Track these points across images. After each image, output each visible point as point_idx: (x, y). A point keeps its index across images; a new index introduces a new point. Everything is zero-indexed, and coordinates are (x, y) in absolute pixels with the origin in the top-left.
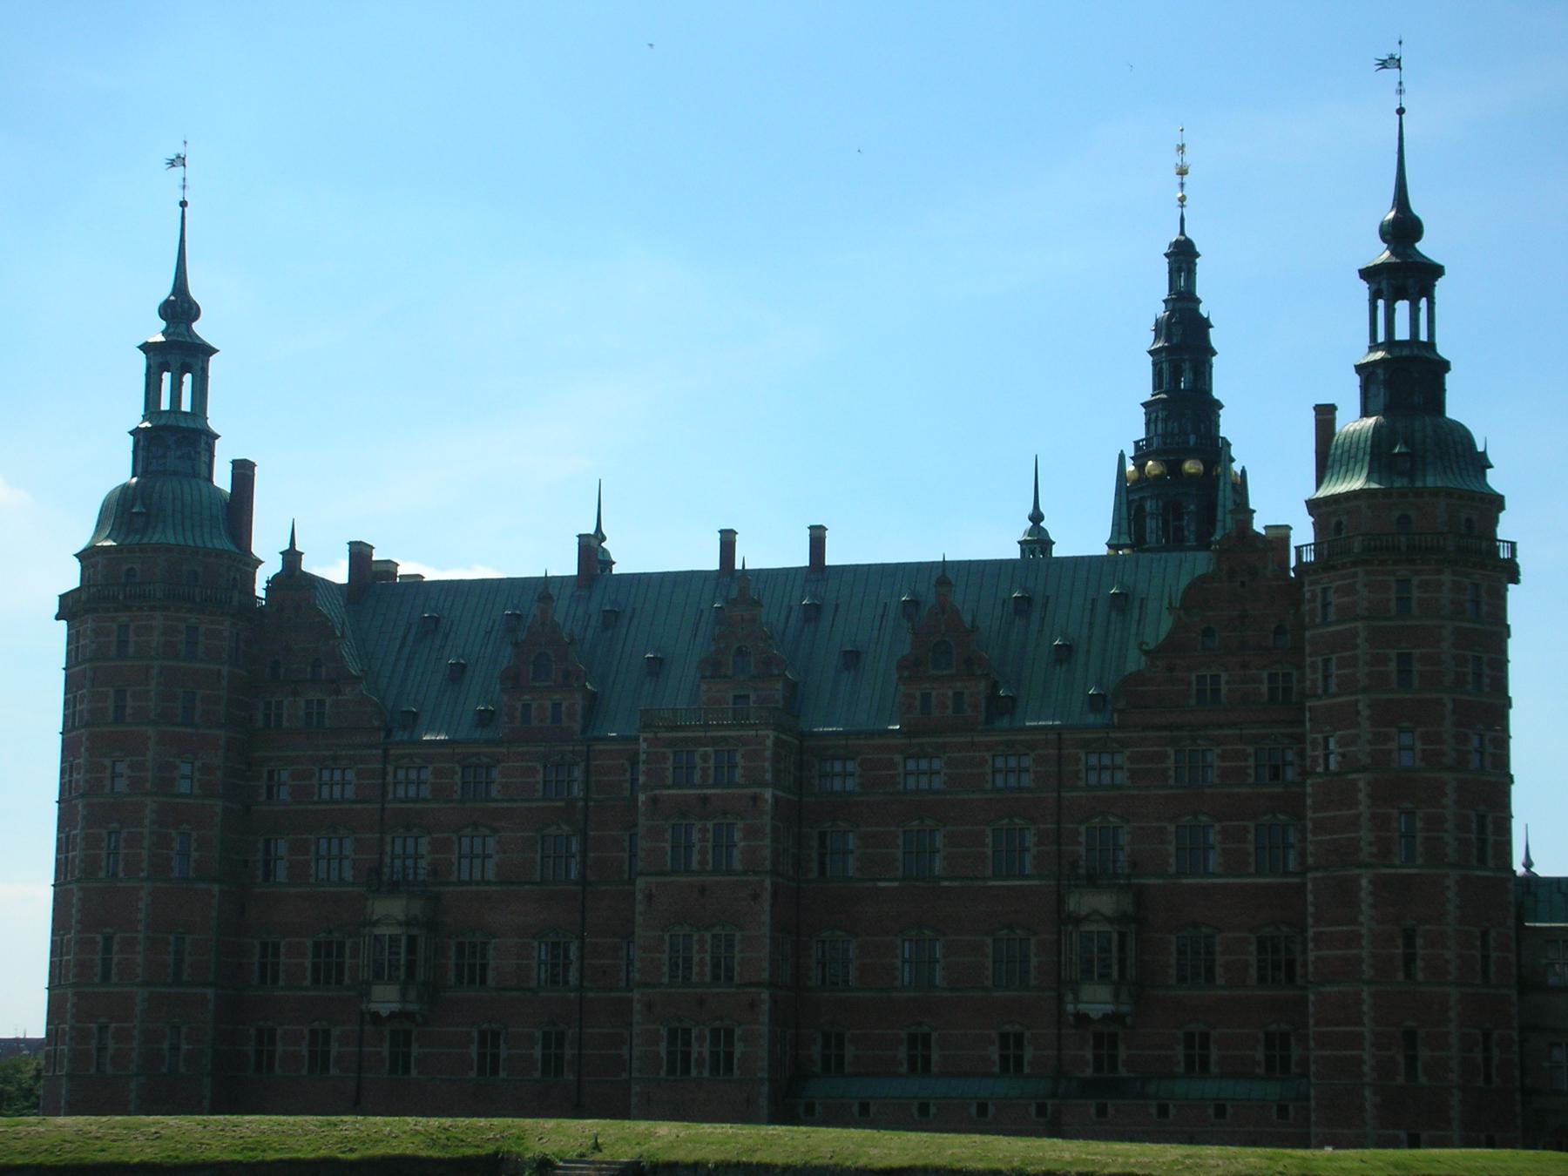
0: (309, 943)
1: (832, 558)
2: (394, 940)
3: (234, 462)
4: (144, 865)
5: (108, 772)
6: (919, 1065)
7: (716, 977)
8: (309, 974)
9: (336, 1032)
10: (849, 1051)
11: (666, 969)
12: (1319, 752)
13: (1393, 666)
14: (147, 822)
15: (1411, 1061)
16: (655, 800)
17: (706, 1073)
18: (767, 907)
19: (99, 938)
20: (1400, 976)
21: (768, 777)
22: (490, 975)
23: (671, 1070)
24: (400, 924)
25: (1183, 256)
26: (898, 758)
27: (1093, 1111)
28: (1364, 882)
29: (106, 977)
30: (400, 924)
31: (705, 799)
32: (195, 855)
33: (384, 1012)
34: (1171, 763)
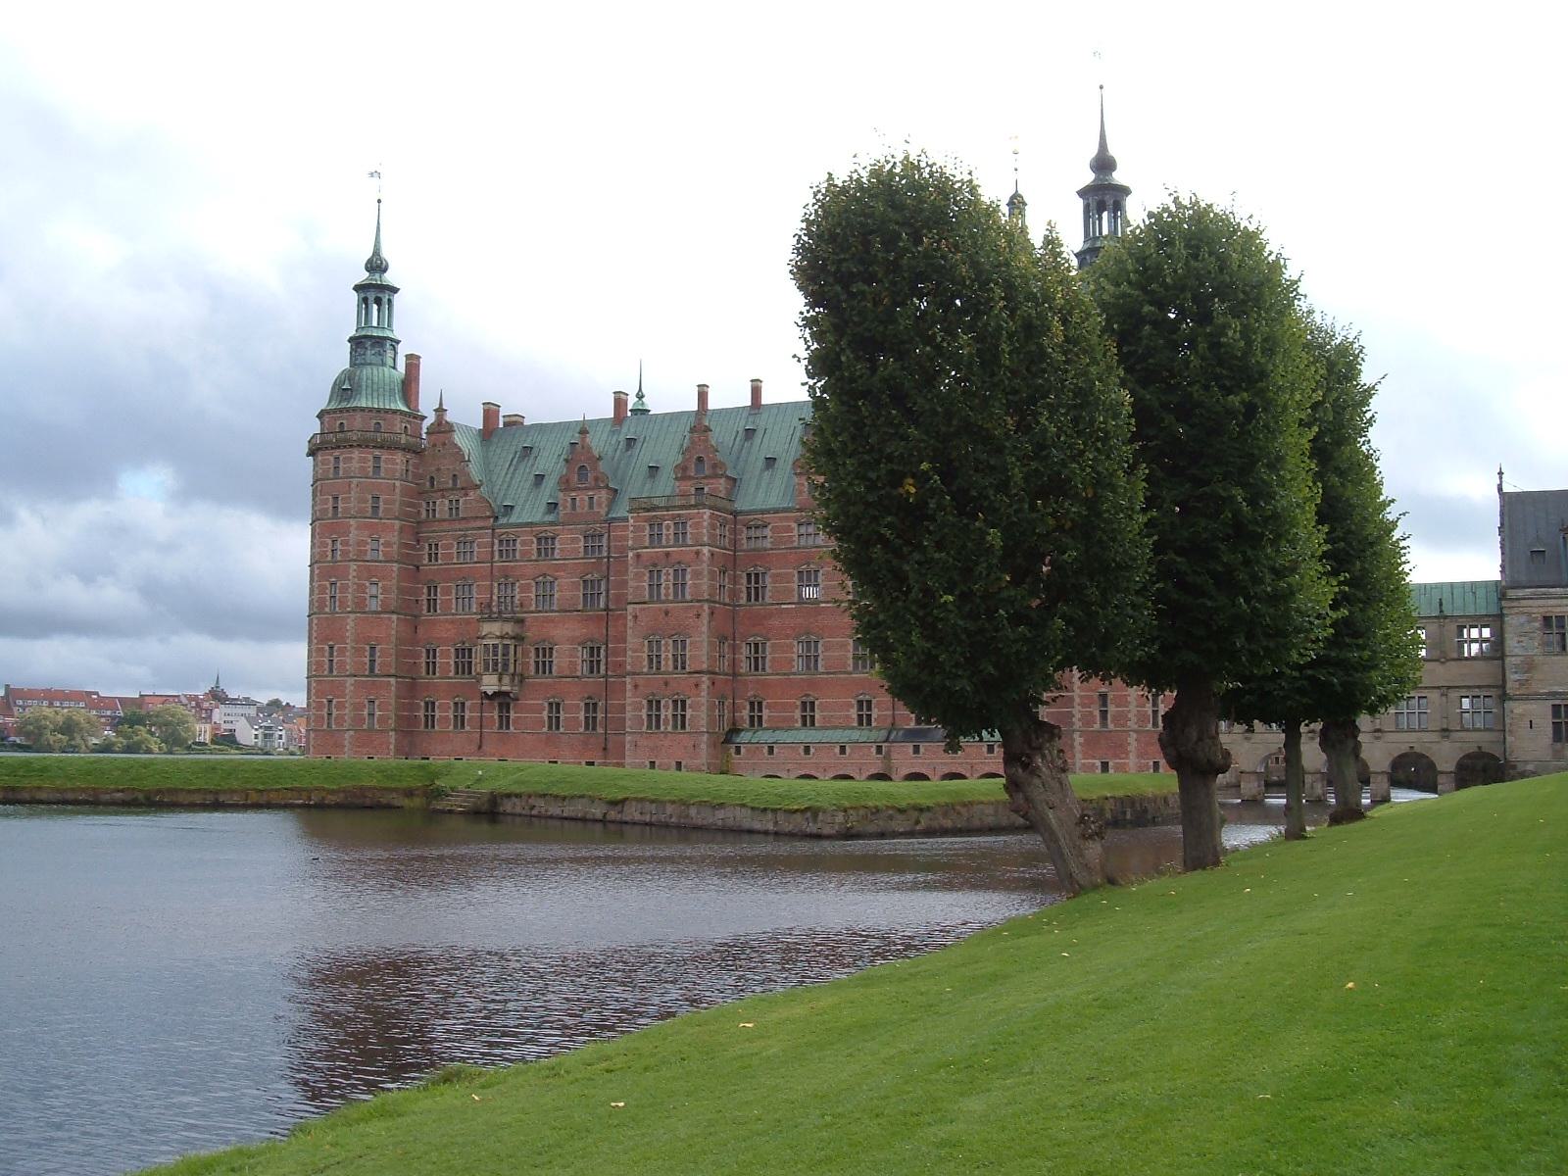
0: (453, 650)
1: (766, 399)
2: (495, 646)
3: (406, 356)
5: (330, 547)
6: (808, 721)
8: (452, 668)
9: (468, 704)
10: (765, 713)
11: (646, 663)
14: (350, 577)
15: (1104, 714)
16: (638, 556)
17: (670, 729)
18: (705, 622)
19: (327, 648)
21: (705, 539)
22: (554, 669)
23: (649, 727)
24: (498, 637)
26: (794, 525)
27: (911, 750)
29: (331, 671)
30: (498, 637)
31: (668, 554)
32: (381, 597)
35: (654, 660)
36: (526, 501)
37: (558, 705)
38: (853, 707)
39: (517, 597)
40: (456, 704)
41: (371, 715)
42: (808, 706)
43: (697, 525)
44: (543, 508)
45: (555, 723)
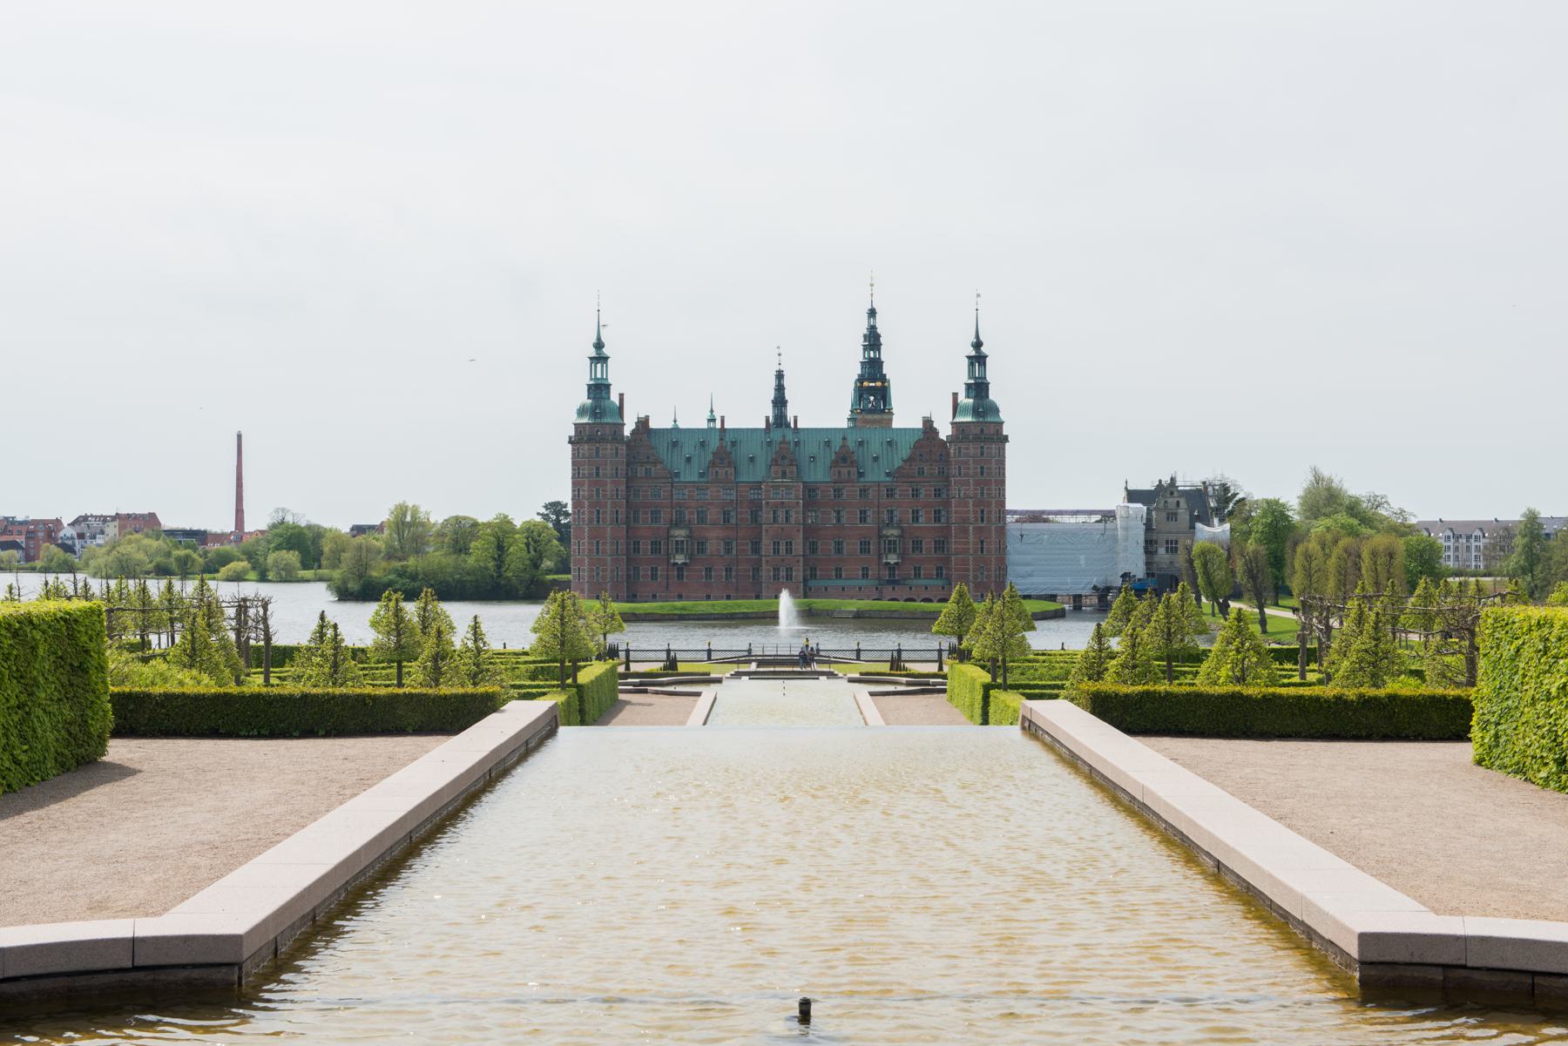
0: (649, 542)
1: (799, 426)
2: (682, 542)
4: (608, 520)
6: (839, 576)
7: (787, 553)
9: (659, 568)
10: (818, 573)
12: (957, 492)
13: (979, 470)
16: (767, 503)
20: (980, 553)
21: (801, 497)
23: (774, 579)
25: (872, 313)
26: (832, 490)
28: (971, 528)
29: (598, 553)
31: (783, 503)
33: (680, 563)
34: (910, 492)
35: (777, 551)
36: (686, 469)
37: (710, 569)
38: (858, 569)
39: (687, 517)
40: (652, 568)
41: (618, 574)
42: (839, 570)
43: (798, 490)
44: (696, 475)
45: (708, 576)
